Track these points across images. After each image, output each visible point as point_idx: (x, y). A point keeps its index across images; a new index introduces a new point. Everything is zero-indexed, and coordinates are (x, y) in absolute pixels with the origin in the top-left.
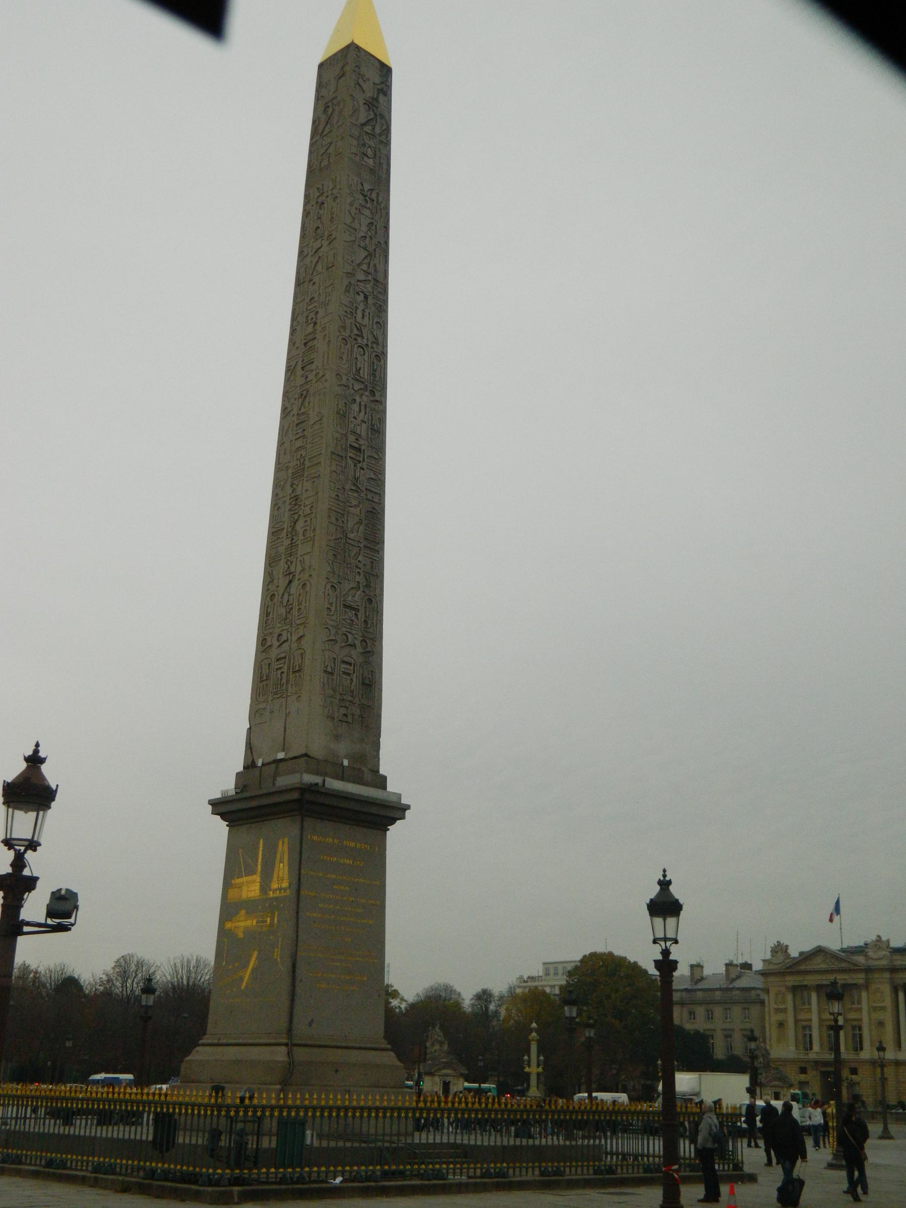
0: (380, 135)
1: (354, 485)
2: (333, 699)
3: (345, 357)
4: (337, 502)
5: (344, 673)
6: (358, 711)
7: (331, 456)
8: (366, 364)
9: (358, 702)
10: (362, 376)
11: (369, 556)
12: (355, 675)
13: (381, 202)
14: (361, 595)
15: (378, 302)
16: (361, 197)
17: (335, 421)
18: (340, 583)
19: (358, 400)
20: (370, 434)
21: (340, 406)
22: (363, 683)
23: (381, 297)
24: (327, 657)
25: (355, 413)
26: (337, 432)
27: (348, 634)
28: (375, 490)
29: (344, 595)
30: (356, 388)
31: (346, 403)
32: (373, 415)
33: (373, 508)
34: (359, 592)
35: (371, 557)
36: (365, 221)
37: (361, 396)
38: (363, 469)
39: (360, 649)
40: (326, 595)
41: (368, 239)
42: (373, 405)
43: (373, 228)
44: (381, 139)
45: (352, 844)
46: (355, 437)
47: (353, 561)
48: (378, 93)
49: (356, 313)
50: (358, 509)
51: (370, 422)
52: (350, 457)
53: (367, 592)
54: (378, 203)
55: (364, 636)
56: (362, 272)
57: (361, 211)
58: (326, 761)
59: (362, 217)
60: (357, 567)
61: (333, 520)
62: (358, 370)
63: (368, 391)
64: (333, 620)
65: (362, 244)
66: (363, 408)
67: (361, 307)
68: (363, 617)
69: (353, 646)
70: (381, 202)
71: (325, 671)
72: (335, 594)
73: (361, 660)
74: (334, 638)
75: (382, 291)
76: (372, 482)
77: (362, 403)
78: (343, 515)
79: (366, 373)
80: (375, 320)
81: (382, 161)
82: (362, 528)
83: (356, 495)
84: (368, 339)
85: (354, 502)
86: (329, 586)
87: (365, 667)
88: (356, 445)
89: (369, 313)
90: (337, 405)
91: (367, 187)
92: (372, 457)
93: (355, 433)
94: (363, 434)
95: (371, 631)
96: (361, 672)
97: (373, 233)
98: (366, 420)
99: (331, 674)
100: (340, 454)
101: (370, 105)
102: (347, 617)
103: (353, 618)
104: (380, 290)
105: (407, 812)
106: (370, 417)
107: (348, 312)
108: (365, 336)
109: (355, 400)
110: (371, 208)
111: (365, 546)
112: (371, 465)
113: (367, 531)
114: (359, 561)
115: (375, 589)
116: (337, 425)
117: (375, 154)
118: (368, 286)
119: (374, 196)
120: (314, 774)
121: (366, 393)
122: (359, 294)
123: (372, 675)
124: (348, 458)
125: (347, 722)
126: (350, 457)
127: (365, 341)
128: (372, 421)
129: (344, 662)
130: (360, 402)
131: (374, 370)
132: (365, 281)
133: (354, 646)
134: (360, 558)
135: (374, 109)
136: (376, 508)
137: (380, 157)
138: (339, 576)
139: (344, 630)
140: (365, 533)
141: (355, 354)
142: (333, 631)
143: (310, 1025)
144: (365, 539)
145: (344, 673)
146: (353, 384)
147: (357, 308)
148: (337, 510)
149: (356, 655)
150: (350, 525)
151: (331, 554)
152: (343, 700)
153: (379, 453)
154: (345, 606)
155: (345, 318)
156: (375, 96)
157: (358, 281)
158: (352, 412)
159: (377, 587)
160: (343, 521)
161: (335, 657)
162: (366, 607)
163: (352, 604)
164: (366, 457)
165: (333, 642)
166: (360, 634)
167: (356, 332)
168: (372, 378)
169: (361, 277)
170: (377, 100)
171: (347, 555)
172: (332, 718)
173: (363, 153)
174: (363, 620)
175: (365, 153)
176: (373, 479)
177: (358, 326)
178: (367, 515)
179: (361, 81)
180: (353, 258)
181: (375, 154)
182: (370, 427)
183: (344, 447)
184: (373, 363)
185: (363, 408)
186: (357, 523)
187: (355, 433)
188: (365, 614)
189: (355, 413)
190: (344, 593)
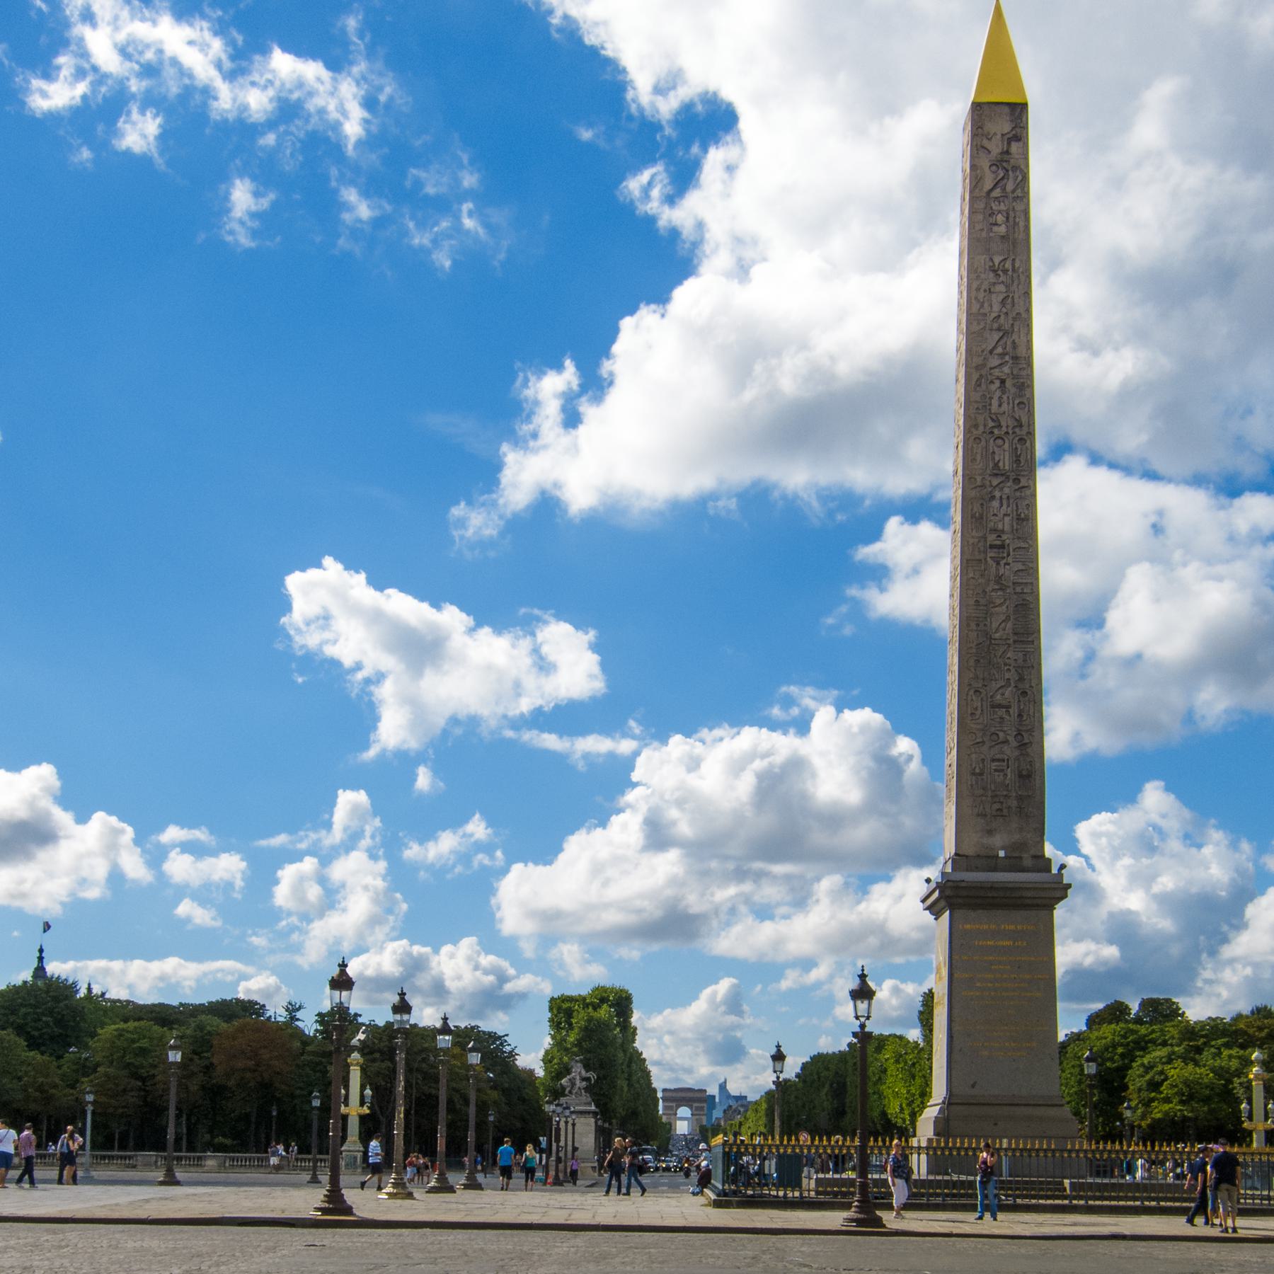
0: (1013, 191)
2: (984, 798)
3: (979, 457)
5: (996, 770)
6: (1015, 802)
7: (967, 563)
8: (1007, 453)
10: (1002, 468)
13: (1019, 268)
14: (1012, 691)
16: (992, 275)
18: (986, 686)
19: (997, 494)
21: (975, 510)
22: (1021, 776)
23: (1024, 373)
26: (973, 537)
28: (1024, 581)
29: (991, 697)
31: (982, 504)
33: (1024, 600)
34: (1010, 689)
37: (1002, 489)
38: (1008, 564)
39: (1015, 744)
41: (1003, 317)
42: (1018, 494)
43: (1010, 300)
44: (1015, 195)
45: (1012, 927)
47: (999, 660)
48: (1009, 144)
49: (990, 405)
50: (1004, 607)
51: (1015, 513)
53: (1020, 686)
54: (1014, 270)
55: (1019, 730)
56: (996, 357)
57: (992, 290)
58: (978, 856)
59: (994, 296)
60: (1006, 664)
62: (996, 465)
65: (995, 326)
66: (1005, 502)
67: (998, 394)
69: (1006, 742)
70: (1019, 268)
71: (973, 774)
73: (1017, 753)
74: (981, 740)
75: (1024, 366)
77: (1004, 497)
78: (986, 618)
80: (1016, 402)
81: (1017, 220)
82: (1009, 625)
83: (1000, 593)
84: (1007, 427)
85: (998, 602)
86: (972, 692)
87: (1021, 759)
88: (998, 543)
89: (1008, 398)
90: (972, 510)
91: (997, 260)
92: (1020, 548)
94: (1007, 528)
95: (1027, 722)
99: (981, 774)
100: (978, 558)
102: (995, 716)
104: (1021, 366)
105: (1069, 891)
106: (1015, 508)
108: (1004, 424)
109: (994, 496)
110: (1005, 280)
111: (1015, 642)
114: (1009, 658)
115: (1031, 680)
116: (972, 530)
117: (1007, 218)
119: (1008, 265)
120: (963, 871)
121: (1009, 484)
122: (993, 383)
123: (1031, 765)
124: (989, 559)
125: (1002, 816)
127: (1004, 429)
128: (1017, 511)
129: (993, 760)
131: (1017, 456)
132: (1002, 364)
133: (1006, 742)
135: (1004, 164)
137: (1015, 217)
138: (983, 679)
139: (993, 729)
143: (973, 1086)
145: (996, 770)
146: (990, 481)
147: (991, 398)
148: (978, 615)
149: (1010, 751)
150: (995, 625)
152: (996, 796)
154: (993, 707)
155: (977, 416)
156: (1005, 149)
157: (991, 369)
158: (991, 510)
160: (985, 625)
161: (983, 756)
162: (1019, 701)
163: (1001, 702)
164: (1011, 550)
166: (1013, 729)
167: (991, 424)
168: (1015, 466)
169: (995, 361)
170: (1007, 152)
171: (993, 656)
172: (983, 815)
173: (991, 224)
176: (1022, 570)
177: (994, 417)
179: (986, 143)
180: (984, 347)
181: (1007, 218)
182: (1015, 517)
183: (982, 549)
184: (1016, 448)
185: (1005, 502)
186: (1003, 621)
187: (995, 530)
188: (1019, 707)
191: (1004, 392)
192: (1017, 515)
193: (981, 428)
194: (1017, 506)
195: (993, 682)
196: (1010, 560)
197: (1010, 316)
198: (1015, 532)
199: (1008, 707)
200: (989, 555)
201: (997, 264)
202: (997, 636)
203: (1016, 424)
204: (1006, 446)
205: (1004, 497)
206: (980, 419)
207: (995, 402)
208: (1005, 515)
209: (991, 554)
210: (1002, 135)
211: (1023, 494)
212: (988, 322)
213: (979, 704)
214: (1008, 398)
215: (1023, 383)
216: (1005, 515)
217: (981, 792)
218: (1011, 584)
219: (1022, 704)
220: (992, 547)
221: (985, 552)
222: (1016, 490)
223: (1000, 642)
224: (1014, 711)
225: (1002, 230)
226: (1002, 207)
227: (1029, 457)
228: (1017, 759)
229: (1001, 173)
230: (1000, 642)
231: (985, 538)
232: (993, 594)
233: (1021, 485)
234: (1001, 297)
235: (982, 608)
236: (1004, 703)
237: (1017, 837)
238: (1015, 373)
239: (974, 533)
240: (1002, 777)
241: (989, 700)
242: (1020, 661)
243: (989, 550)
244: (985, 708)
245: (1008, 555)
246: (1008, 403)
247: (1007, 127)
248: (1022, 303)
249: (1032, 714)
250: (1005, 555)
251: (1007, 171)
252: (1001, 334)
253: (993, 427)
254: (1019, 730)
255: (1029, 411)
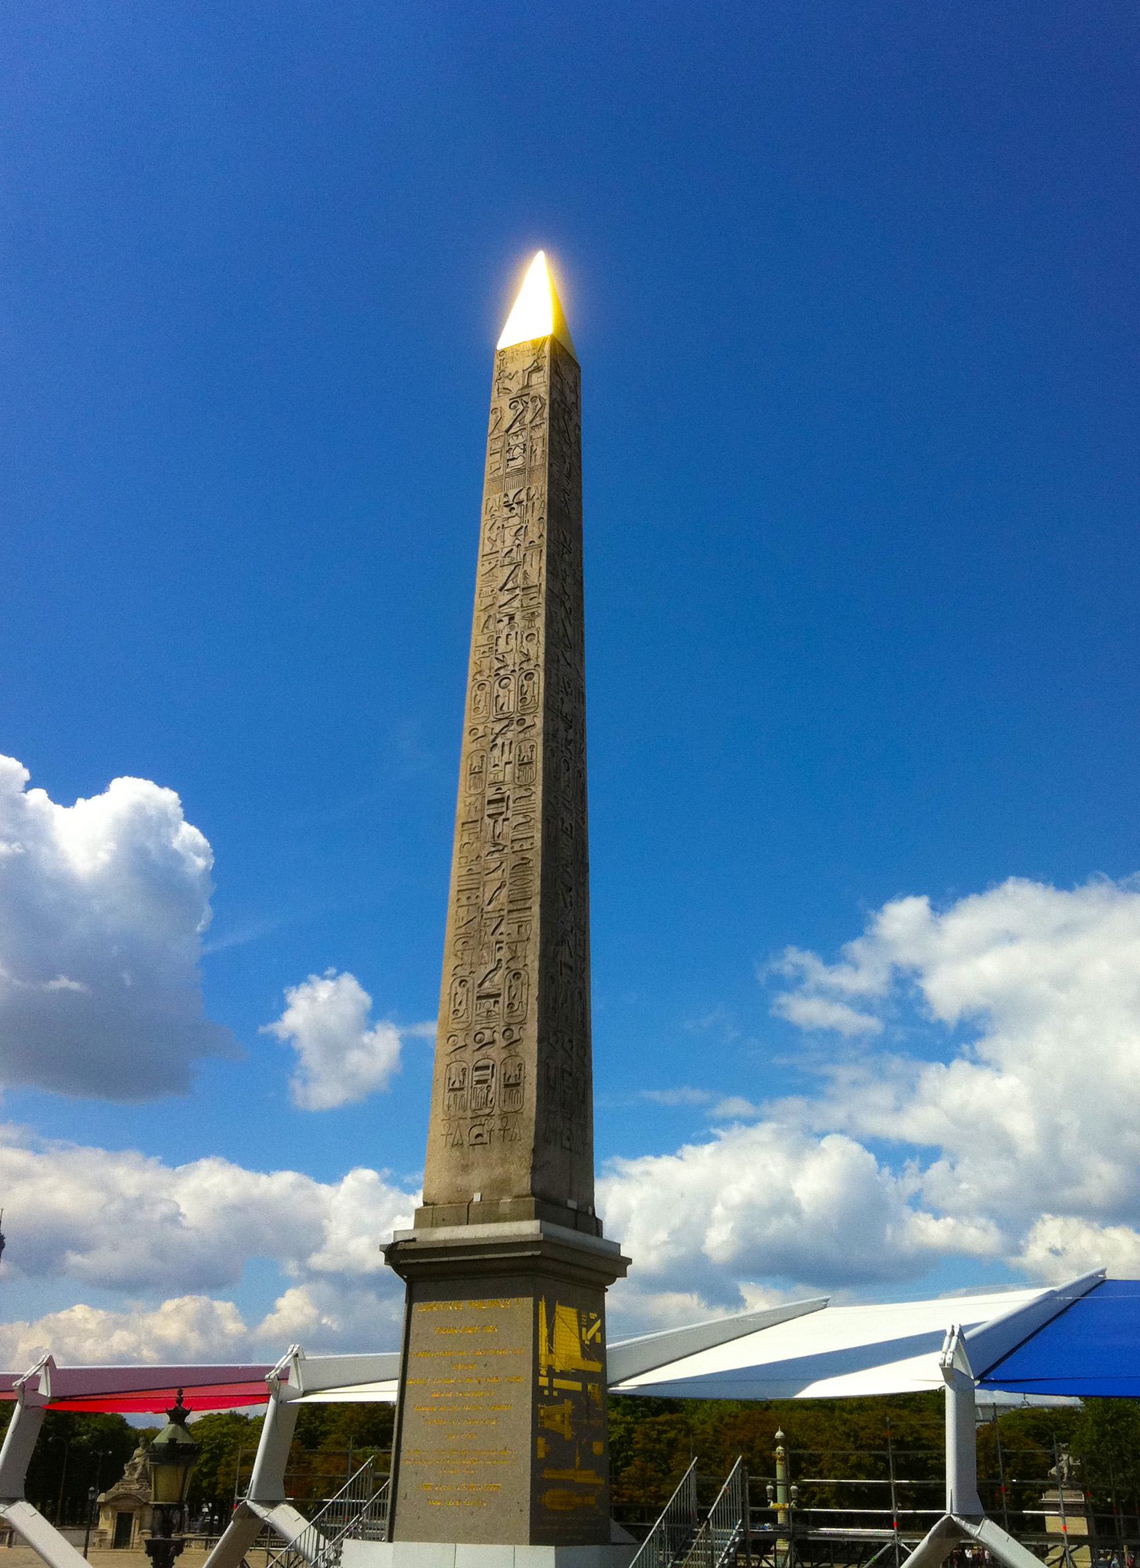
0: (531, 422)
1: (495, 845)
2: (461, 1121)
4: (472, 877)
5: (478, 1082)
9: (498, 1112)
11: (515, 921)
12: (494, 1079)
14: (503, 973)
15: (529, 611)
16: (506, 510)
17: (468, 783)
20: (517, 771)
22: (506, 1086)
24: (453, 1071)
25: (496, 760)
26: (471, 795)
27: (483, 1031)
28: (525, 836)
29: (480, 985)
30: (497, 730)
32: (522, 747)
33: (523, 859)
35: (519, 919)
36: (509, 535)
40: (453, 995)
42: (522, 736)
44: (534, 424)
46: (496, 788)
47: (493, 939)
49: (496, 645)
50: (500, 872)
52: (488, 815)
59: (507, 531)
61: (464, 901)
63: (515, 722)
64: (464, 1022)
65: (507, 560)
66: (506, 748)
68: (507, 999)
72: (465, 989)
74: (464, 1044)
75: (536, 595)
76: (520, 828)
78: (479, 888)
79: (511, 703)
80: (525, 636)
81: (534, 449)
83: (496, 855)
84: (514, 664)
85: (494, 866)
88: (498, 796)
89: (517, 633)
91: (511, 494)
93: (496, 783)
96: (503, 1072)
97: (521, 538)
98: (511, 759)
100: (474, 819)
101: (515, 400)
102: (482, 1010)
103: (492, 1008)
104: (532, 596)
106: (518, 753)
107: (487, 650)
108: (510, 662)
111: (510, 911)
112: (519, 808)
113: (513, 892)
114: (501, 934)
115: (525, 957)
116: (470, 787)
117: (525, 450)
118: (512, 604)
121: (512, 728)
122: (502, 621)
125: (482, 1144)
126: (488, 815)
127: (511, 668)
128: (519, 755)
129: (477, 1069)
130: (504, 743)
134: (502, 929)
136: (527, 856)
138: (471, 964)
139: (478, 1027)
140: (509, 896)
141: (495, 691)
142: (461, 1035)
144: (511, 902)
145: (478, 1082)
149: (495, 1054)
150: (488, 896)
151: (460, 943)
153: (531, 787)
154: (479, 998)
157: (500, 607)
158: (492, 760)
159: (528, 953)
161: (464, 1065)
163: (490, 991)
165: (464, 1048)
167: (497, 665)
169: (504, 597)
170: (528, 386)
171: (483, 934)
172: (458, 1145)
173: (508, 460)
174: (506, 1005)
175: (511, 457)
178: (513, 871)
183: (479, 808)
187: (496, 783)
189: (496, 760)
190: (479, 982)
191: (512, 628)
192: (519, 761)
193: (486, 673)
194: (520, 750)
195: (483, 966)
196: (509, 814)
197: (522, 548)
198: (516, 780)
199: (499, 995)
200: (486, 814)
201: (511, 500)
202: (490, 908)
203: (524, 659)
204: (512, 687)
205: (507, 742)
206: (486, 662)
207: (502, 642)
208: (506, 763)
209: (490, 810)
210: (523, 371)
211: (528, 735)
212: (500, 559)
213: (465, 996)
214: (517, 633)
215: (533, 613)
216: (506, 763)
217: (460, 1113)
218: (509, 843)
219: (513, 989)
220: (490, 802)
221: (482, 810)
222: (520, 732)
223: (493, 915)
224: (504, 1000)
225: (519, 462)
226: (521, 439)
227: (536, 692)
228: (503, 1062)
229: (521, 407)
230: (493, 915)
231: (483, 794)
232: (489, 857)
233: (526, 725)
234: (515, 529)
235: (475, 877)
236: (495, 991)
237: (498, 1171)
238: (525, 605)
239: (473, 791)
240: (485, 1090)
241: (476, 990)
242: (514, 935)
243: (487, 807)
244: (470, 1003)
245: (507, 809)
246: (516, 639)
247: (528, 362)
248: (536, 529)
249: (525, 1001)
250: (504, 809)
251: (527, 403)
252: (512, 567)
253: (499, 669)
254: (510, 1024)
255: (538, 641)
